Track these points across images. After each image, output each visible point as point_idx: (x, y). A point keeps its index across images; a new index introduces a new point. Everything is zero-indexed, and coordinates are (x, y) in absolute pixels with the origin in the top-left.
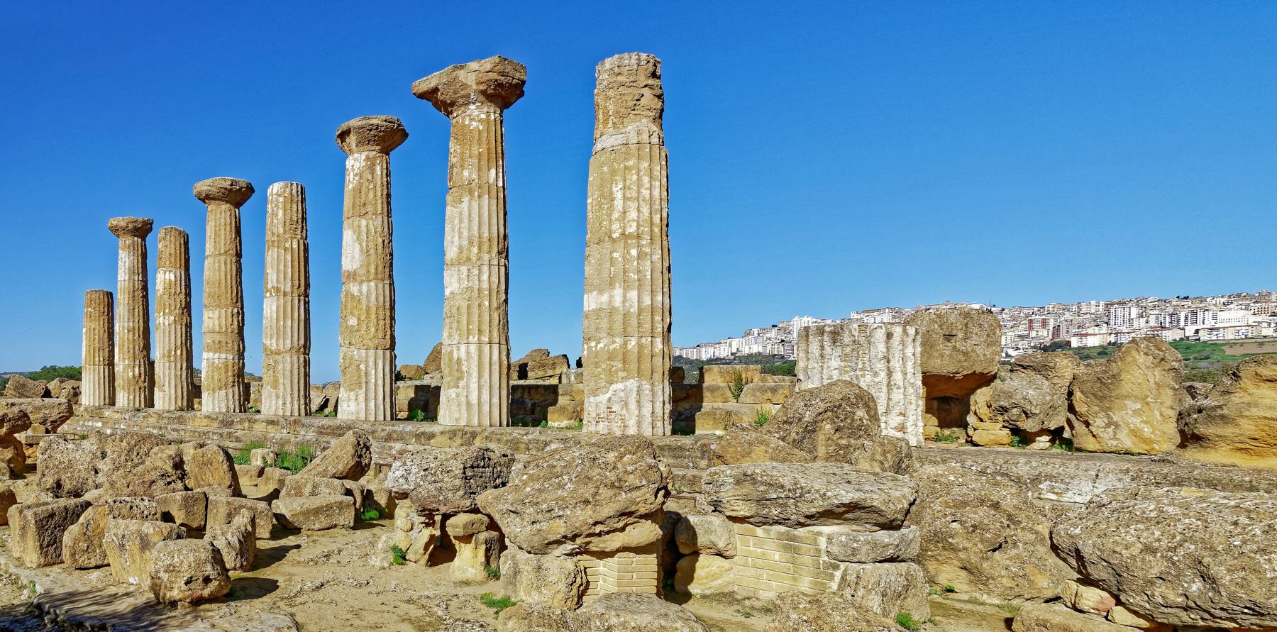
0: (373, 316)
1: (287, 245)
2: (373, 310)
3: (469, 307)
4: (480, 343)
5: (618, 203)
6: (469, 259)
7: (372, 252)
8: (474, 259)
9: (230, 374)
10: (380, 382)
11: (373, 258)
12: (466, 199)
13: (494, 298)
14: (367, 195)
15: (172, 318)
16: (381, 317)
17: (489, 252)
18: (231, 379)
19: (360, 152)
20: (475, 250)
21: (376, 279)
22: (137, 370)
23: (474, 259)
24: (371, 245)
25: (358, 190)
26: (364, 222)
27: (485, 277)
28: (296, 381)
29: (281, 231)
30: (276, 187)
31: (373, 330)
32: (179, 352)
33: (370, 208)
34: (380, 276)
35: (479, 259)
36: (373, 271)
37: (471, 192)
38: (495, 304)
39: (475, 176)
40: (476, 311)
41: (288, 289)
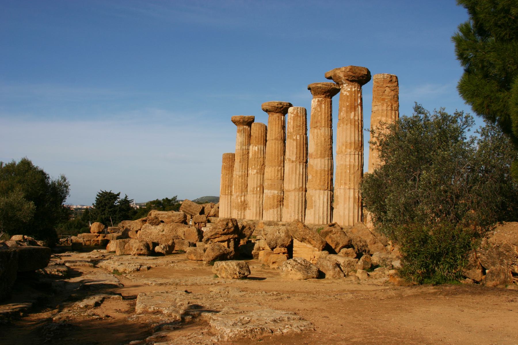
0: (319, 175)
1: (295, 138)
2: (319, 172)
3: (341, 173)
4: (345, 189)
6: (342, 152)
7: (319, 144)
9: (276, 201)
10: (321, 206)
11: (319, 147)
12: (342, 125)
13: (352, 169)
14: (318, 118)
15: (255, 171)
16: (323, 175)
17: (350, 149)
18: (276, 203)
19: (315, 98)
20: (344, 148)
21: (320, 157)
22: (243, 198)
23: (344, 151)
24: (319, 141)
25: (314, 116)
26: (316, 131)
27: (348, 160)
28: (297, 205)
29: (292, 130)
31: (318, 181)
32: (258, 189)
33: (318, 124)
34: (323, 156)
35: (346, 152)
36: (319, 153)
37: (343, 123)
38: (352, 172)
39: (345, 115)
40: (344, 175)
41: (294, 159)
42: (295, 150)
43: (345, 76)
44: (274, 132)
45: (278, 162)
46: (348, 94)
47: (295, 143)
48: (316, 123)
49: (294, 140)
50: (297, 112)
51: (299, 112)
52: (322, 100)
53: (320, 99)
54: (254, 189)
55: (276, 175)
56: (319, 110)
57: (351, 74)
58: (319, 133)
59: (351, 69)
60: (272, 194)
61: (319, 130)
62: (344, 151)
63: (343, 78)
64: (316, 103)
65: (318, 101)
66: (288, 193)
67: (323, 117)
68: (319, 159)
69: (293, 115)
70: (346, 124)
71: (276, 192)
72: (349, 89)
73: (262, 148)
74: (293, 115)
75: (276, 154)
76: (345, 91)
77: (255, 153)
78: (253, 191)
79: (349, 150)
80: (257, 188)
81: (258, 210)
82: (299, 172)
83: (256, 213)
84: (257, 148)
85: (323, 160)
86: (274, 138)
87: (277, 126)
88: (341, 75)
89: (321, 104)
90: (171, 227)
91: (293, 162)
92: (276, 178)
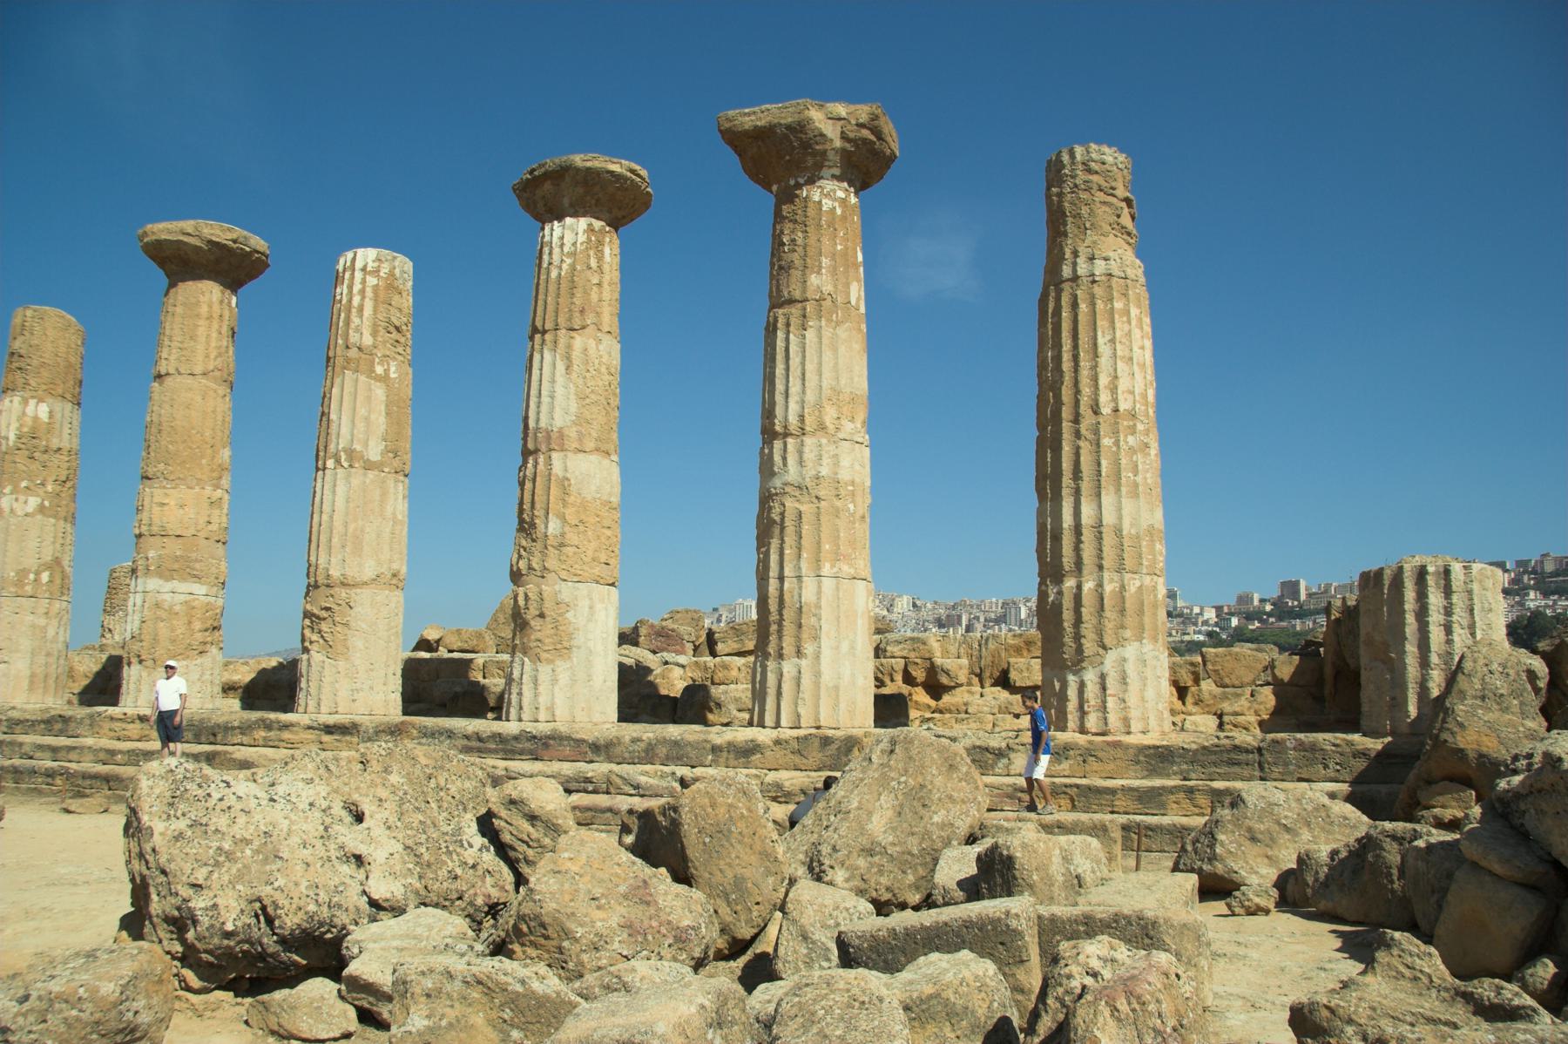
5: (1104, 361)
6: (822, 427)
8: (831, 427)
9: (197, 625)
14: (586, 293)
15: (33, 502)
17: (852, 420)
19: (575, 215)
26: (578, 341)
29: (368, 340)
30: (367, 256)
32: (45, 577)
42: (382, 419)
43: (844, 137)
44: (200, 348)
45: (212, 471)
46: (839, 211)
47: (380, 392)
48: (582, 311)
49: (378, 379)
50: (391, 274)
51: (397, 272)
52: (602, 231)
53: (598, 224)
54: (23, 573)
55: (202, 521)
56: (593, 263)
57: (866, 133)
58: (592, 351)
59: (875, 118)
60: (182, 598)
61: (592, 343)
62: (828, 421)
63: (838, 143)
64: (582, 238)
65: (590, 229)
66: (342, 593)
67: (606, 295)
68: (594, 458)
69: (372, 281)
70: (838, 323)
71: (200, 589)
72: (841, 194)
73: (67, 413)
74: (372, 281)
75: (208, 433)
76: (828, 195)
77: (34, 429)
78: (20, 583)
79: (848, 427)
80: (38, 573)
81: (41, 659)
82: (394, 514)
83: (33, 676)
84: (43, 411)
85: (606, 462)
86: (198, 369)
87: (215, 325)
88: (831, 131)
89: (600, 243)
90: (394, 778)
91: (369, 466)
92: (202, 534)
